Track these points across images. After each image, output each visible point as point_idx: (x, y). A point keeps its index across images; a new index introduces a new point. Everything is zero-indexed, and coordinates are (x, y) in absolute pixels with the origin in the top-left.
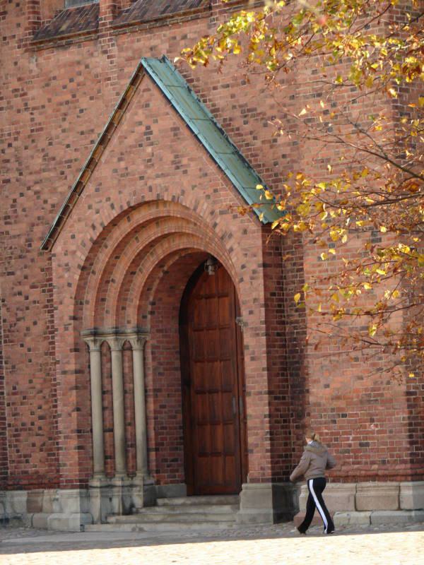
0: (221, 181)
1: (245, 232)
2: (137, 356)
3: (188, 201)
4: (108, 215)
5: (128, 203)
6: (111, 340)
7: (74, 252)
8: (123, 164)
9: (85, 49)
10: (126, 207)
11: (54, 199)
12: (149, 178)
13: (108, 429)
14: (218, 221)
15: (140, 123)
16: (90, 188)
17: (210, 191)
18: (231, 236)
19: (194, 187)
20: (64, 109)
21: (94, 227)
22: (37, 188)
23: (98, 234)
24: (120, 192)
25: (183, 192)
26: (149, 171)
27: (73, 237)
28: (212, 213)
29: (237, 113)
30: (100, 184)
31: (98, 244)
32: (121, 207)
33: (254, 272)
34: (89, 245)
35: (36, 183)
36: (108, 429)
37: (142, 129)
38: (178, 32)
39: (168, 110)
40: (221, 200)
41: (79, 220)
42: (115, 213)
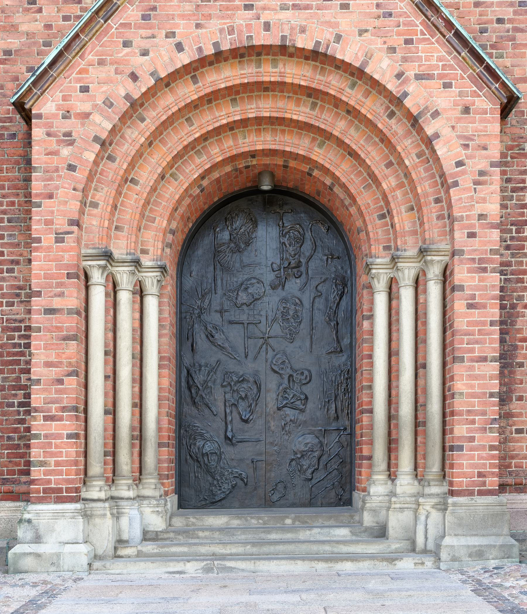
0: (421, 27)
1: (466, 110)
5: (216, 45)
10: (209, 51)
12: (264, 8)
17: (398, 41)
18: (436, 114)
19: (361, 32)
21: (134, 77)
23: (144, 90)
24: (198, 26)
25: (338, 38)
27: (85, 89)
28: (399, 76)
30: (154, 9)
32: (200, 49)
33: (482, 173)
34: (123, 106)
40: (420, 58)
41: (101, 63)
42: (184, 59)
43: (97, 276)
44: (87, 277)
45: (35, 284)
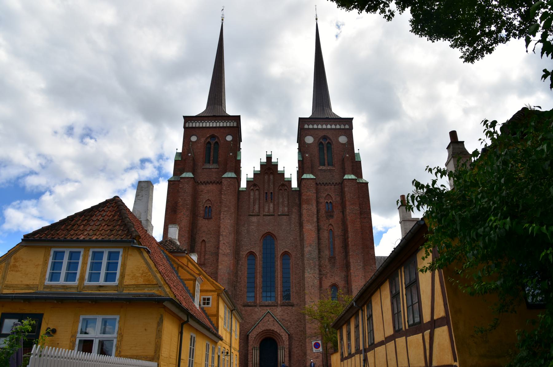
1: (285, 335)
2: (258, 351)
3: (275, 330)
4: (260, 331)
6: (256, 349)
7: (253, 335)
8: (263, 324)
9: (254, 308)
11: (246, 327)
13: (255, 361)
14: (281, 333)
15: (267, 319)
16: (257, 327)
20: (249, 315)
22: (243, 325)
26: (268, 325)
29: (281, 319)
31: (257, 335)
35: (243, 325)
36: (255, 361)
37: (268, 320)
38: (271, 308)
39: (272, 317)
42: (261, 331)
43: (254, 349)
44: (253, 349)
45: (249, 350)
